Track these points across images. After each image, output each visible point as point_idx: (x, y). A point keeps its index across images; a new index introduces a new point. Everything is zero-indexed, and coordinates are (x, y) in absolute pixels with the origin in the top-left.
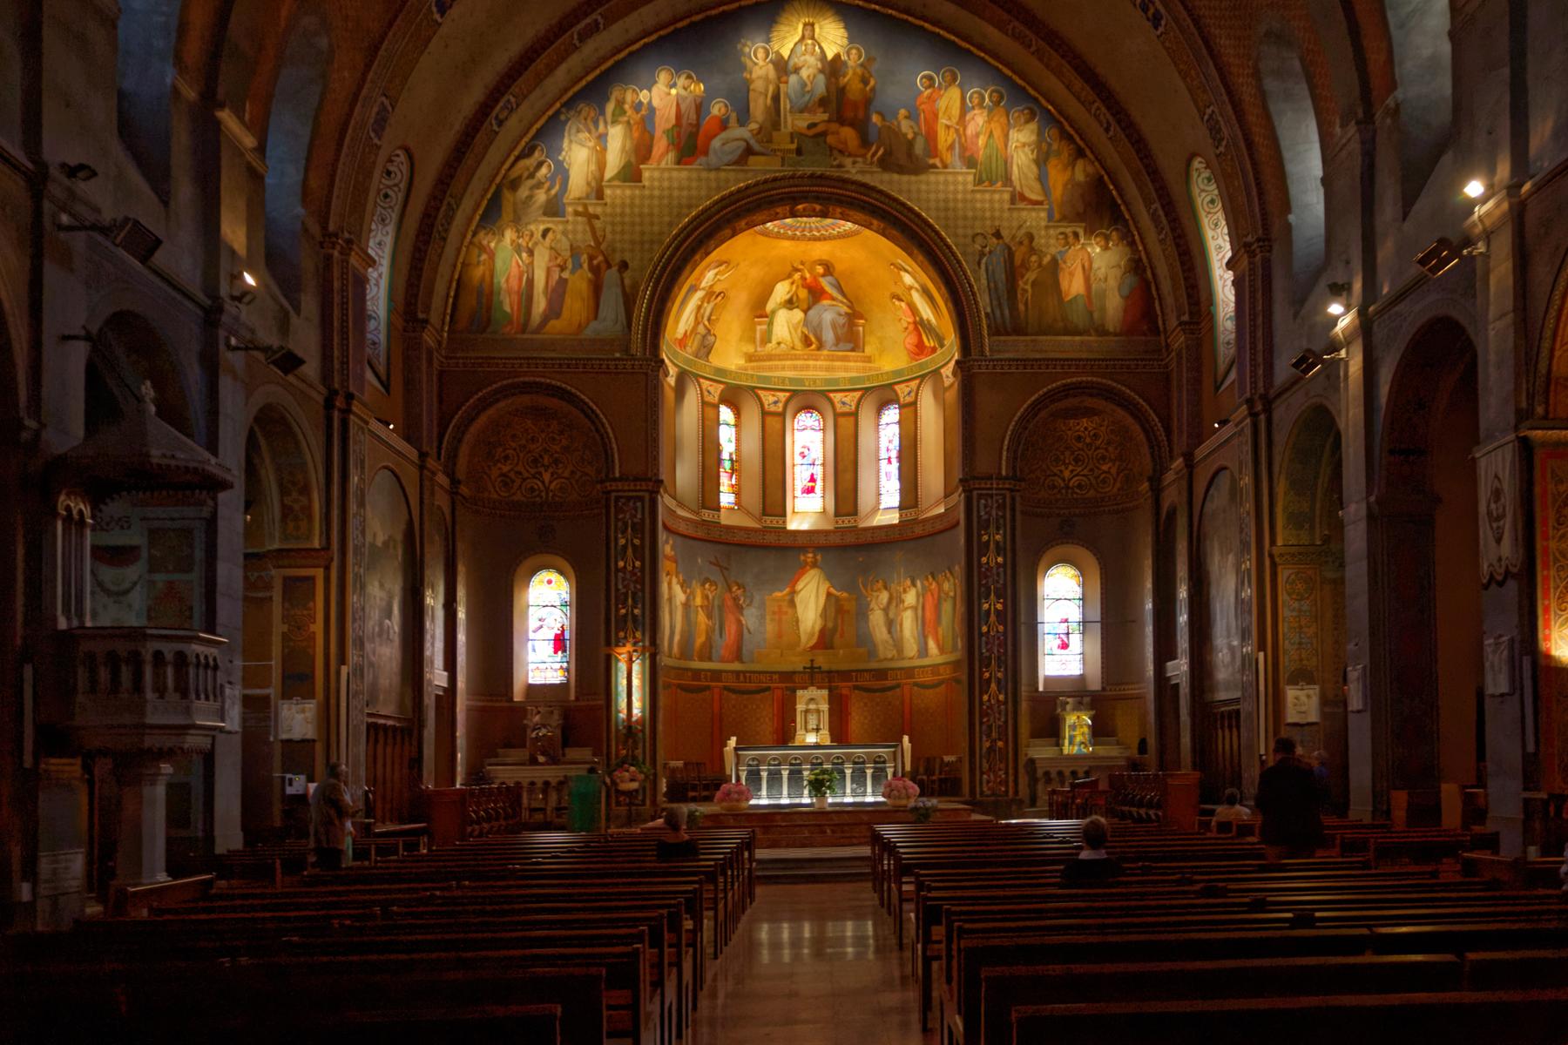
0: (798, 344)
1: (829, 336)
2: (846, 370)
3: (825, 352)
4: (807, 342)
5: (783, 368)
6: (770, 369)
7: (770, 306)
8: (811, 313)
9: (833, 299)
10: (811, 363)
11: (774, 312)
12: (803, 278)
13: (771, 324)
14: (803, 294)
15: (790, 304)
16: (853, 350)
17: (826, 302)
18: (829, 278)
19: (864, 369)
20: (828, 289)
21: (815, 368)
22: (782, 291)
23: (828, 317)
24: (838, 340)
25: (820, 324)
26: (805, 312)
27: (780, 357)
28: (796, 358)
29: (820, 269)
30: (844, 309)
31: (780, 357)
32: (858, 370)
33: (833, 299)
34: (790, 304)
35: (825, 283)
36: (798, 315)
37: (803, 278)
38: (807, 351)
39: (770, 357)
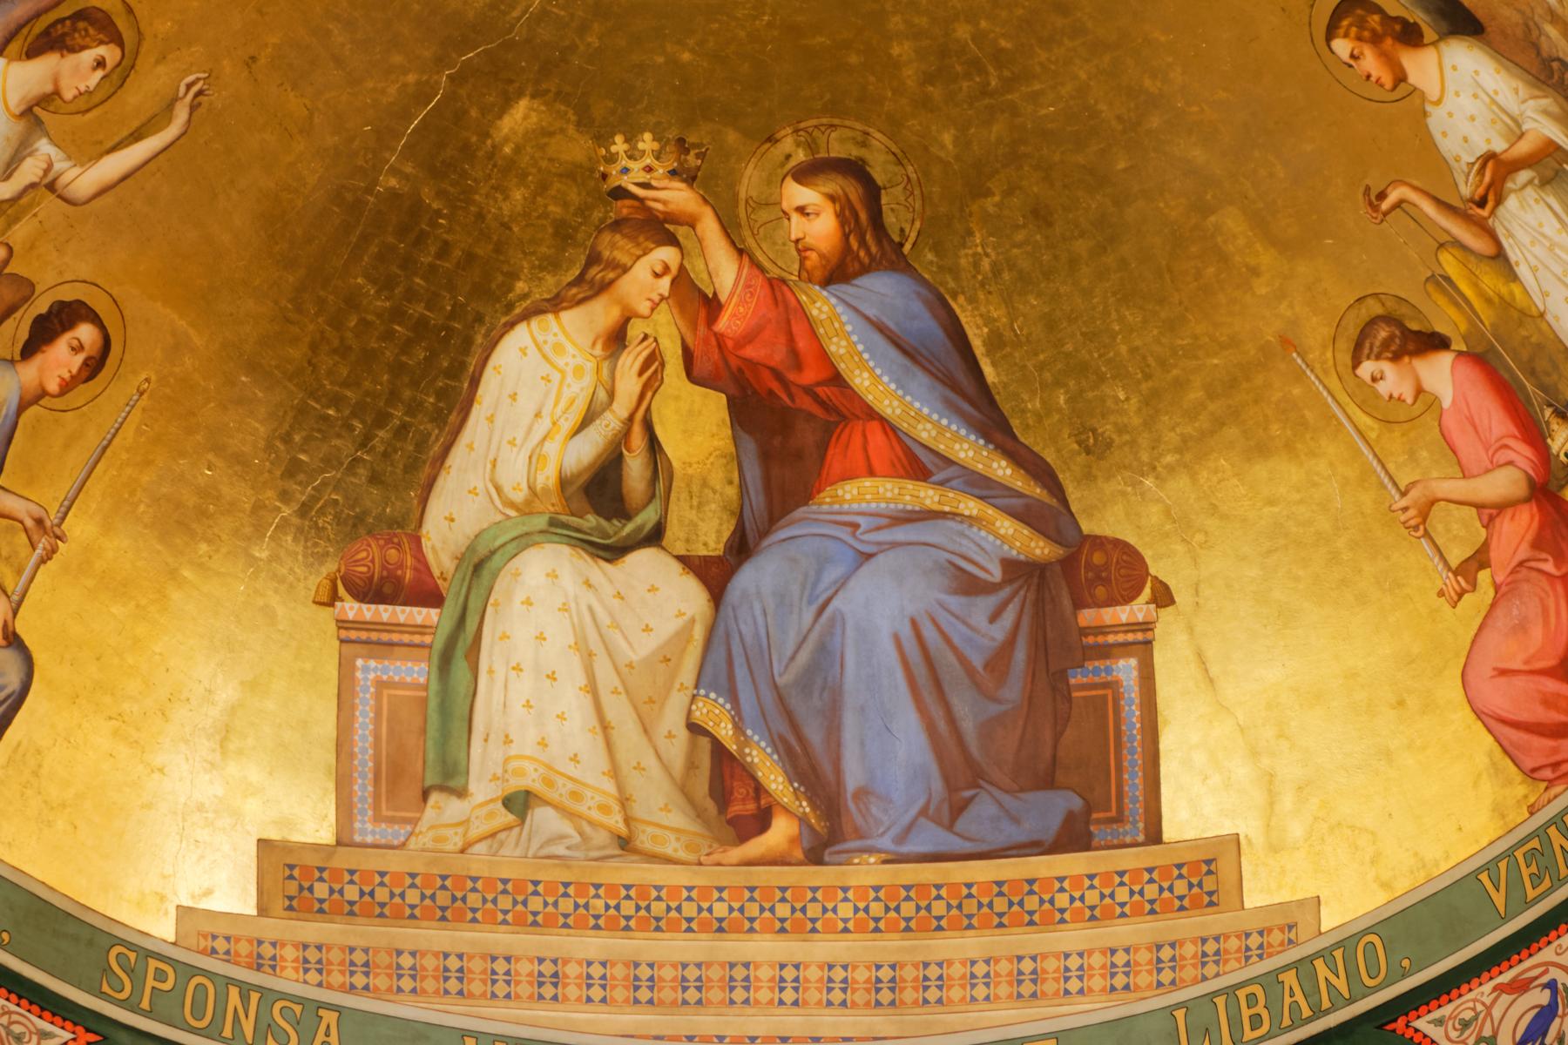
0: (667, 819)
1: (888, 751)
2: (1028, 982)
3: (866, 872)
4: (727, 797)
5: (549, 982)
6: (453, 976)
7: (455, 514)
8: (751, 579)
9: (916, 464)
10: (764, 949)
11: (479, 565)
12: (696, 301)
13: (459, 652)
14: (696, 428)
15: (605, 505)
16: (1073, 838)
17: (864, 494)
18: (882, 291)
19: (1164, 957)
20: (879, 383)
21: (789, 983)
22: (537, 393)
23: (883, 605)
24: (961, 777)
25: (822, 672)
26: (716, 574)
27: (520, 902)
28: (645, 912)
29: (813, 217)
30: (1013, 538)
31: (520, 902)
32: (1119, 971)
33: (916, 464)
34: (605, 505)
35: (851, 335)
36: (656, 598)
37: (696, 301)
38: (730, 869)
39: (449, 898)
